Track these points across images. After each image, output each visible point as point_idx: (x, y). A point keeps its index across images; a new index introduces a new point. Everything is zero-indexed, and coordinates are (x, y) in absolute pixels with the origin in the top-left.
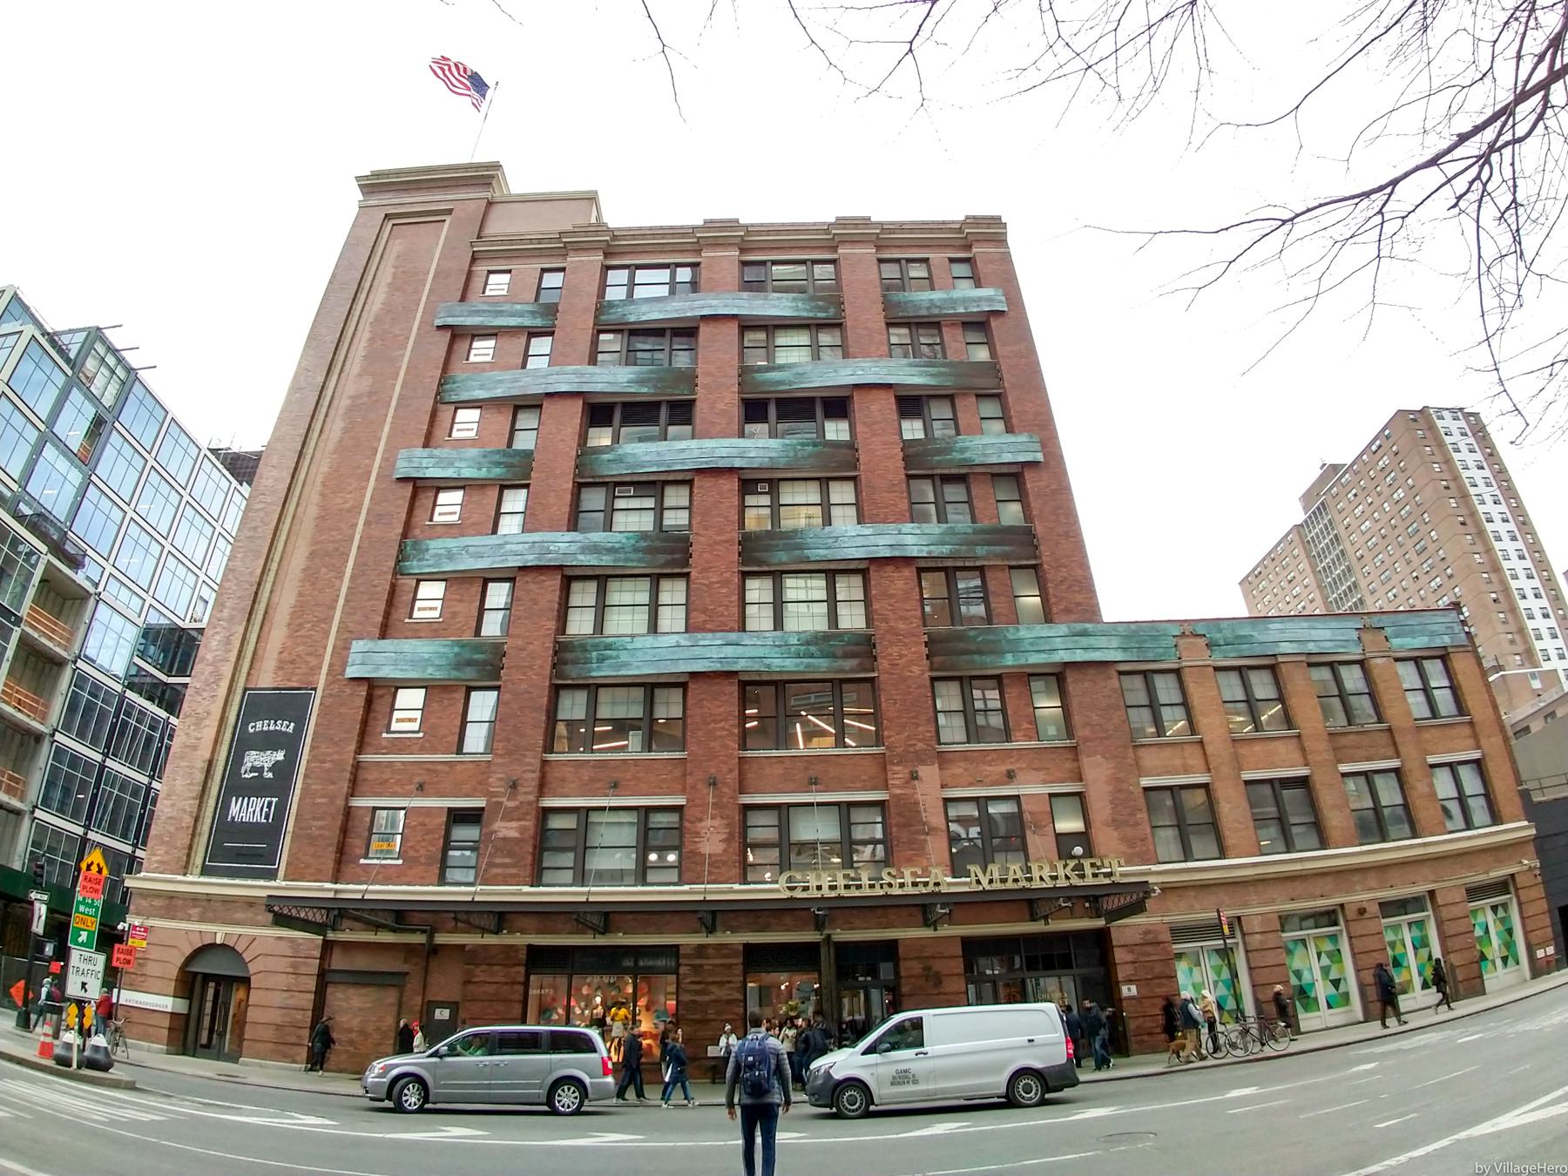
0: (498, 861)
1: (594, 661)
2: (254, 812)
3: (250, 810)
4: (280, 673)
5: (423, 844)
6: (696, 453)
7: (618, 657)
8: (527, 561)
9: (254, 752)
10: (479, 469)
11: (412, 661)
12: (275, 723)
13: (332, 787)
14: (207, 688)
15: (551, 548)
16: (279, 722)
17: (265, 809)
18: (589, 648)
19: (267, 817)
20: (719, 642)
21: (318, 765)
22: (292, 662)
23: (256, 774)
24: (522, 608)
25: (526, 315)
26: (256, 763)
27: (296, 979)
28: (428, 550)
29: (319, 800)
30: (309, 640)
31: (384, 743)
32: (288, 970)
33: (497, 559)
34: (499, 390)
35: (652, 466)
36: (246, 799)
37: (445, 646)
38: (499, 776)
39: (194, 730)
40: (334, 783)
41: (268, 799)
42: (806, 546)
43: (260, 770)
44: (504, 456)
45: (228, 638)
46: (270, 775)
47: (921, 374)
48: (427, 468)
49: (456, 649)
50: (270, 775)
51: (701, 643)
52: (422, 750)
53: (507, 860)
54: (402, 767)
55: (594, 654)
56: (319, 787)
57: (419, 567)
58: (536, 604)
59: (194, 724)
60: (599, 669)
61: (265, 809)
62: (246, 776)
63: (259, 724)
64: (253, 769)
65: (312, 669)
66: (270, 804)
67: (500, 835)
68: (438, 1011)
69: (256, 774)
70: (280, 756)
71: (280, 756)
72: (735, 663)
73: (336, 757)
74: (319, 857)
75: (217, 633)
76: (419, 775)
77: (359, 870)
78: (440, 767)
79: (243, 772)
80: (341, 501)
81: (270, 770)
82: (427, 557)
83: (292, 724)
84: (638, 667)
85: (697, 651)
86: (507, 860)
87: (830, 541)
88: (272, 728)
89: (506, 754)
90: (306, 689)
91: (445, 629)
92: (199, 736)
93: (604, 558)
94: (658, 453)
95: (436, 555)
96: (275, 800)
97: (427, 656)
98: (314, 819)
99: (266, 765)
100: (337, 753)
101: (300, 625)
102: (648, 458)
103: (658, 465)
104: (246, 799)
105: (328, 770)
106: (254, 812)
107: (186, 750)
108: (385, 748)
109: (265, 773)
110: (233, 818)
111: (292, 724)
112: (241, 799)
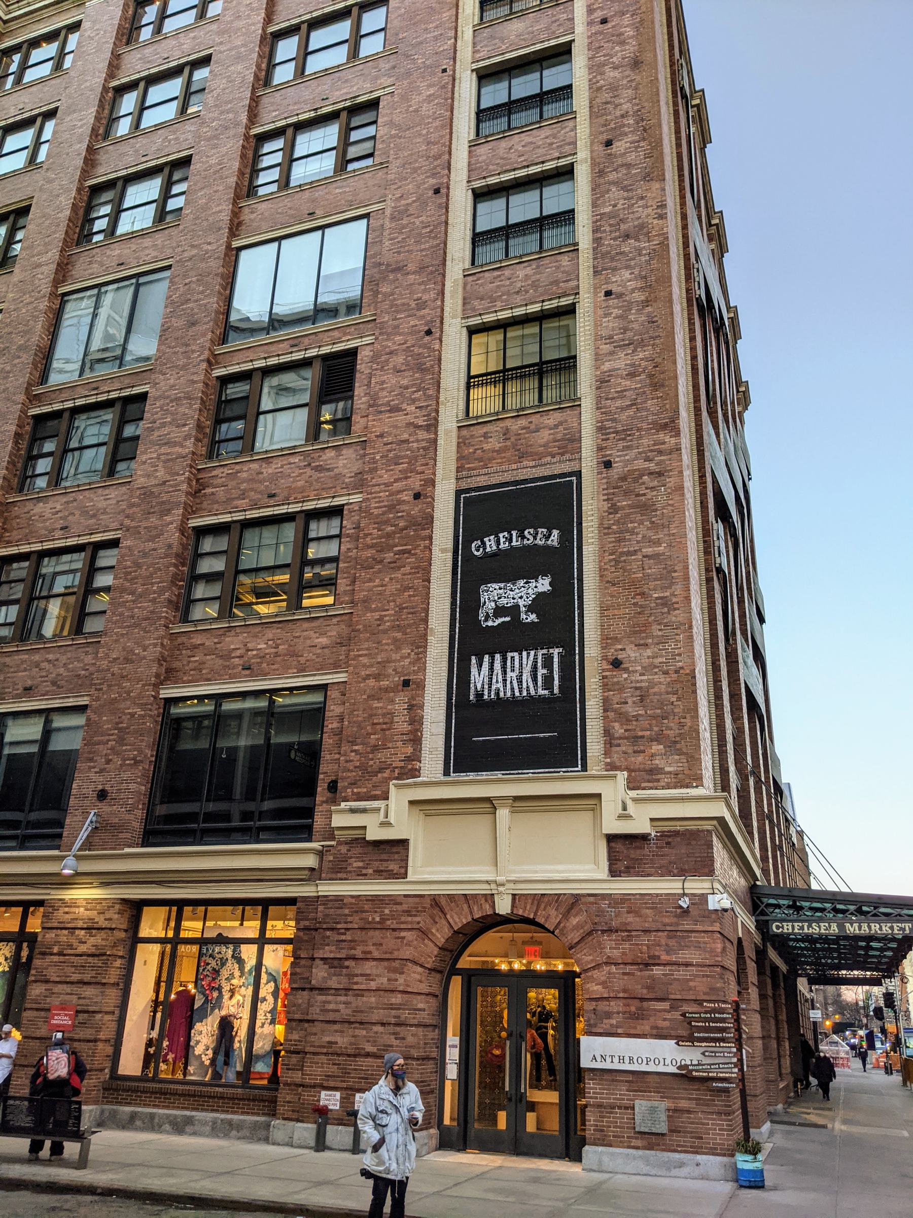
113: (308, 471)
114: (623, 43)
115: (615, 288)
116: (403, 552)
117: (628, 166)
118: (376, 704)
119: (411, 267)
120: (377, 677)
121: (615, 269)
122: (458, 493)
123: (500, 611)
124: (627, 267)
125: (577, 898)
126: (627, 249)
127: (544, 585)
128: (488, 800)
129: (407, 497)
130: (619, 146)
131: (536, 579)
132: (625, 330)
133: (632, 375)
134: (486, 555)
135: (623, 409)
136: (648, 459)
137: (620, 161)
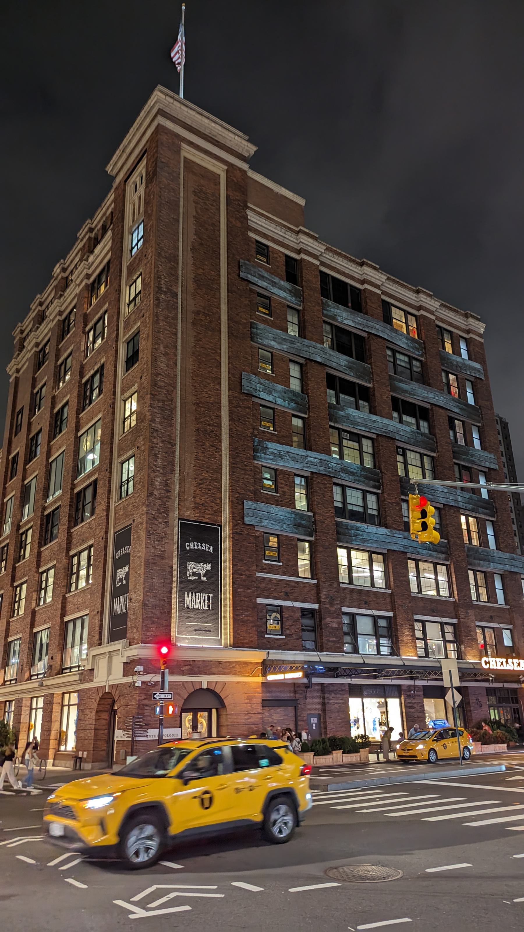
0: (331, 639)
1: (353, 535)
2: (200, 602)
3: (198, 601)
4: (197, 511)
5: (293, 627)
6: (380, 425)
7: (362, 535)
8: (320, 470)
9: (193, 563)
10: (285, 401)
11: (275, 519)
12: (201, 545)
13: (249, 591)
14: (160, 516)
15: (329, 465)
16: (204, 544)
17: (206, 601)
18: (349, 528)
19: (208, 606)
20: (401, 536)
21: (238, 576)
22: (203, 505)
23: (197, 578)
24: (319, 498)
25: (287, 292)
26: (195, 570)
27: (251, 706)
28: (268, 449)
29: (244, 599)
30: (209, 492)
31: (265, 567)
32: (246, 701)
33: (305, 465)
34: (285, 346)
35: (363, 426)
36: (194, 594)
37: (288, 513)
38: (325, 593)
39: (158, 545)
40: (249, 588)
41: (207, 595)
42: (424, 492)
43: (199, 575)
44: (293, 395)
45: (166, 481)
46: (205, 579)
47: (457, 407)
48: (260, 391)
49: (293, 516)
50: (205, 579)
51: (395, 535)
52: (283, 574)
53: (334, 639)
54: (275, 582)
55: (353, 531)
56: (242, 590)
57: (265, 459)
58: (324, 497)
59: (159, 541)
60: (356, 540)
61: (206, 601)
62: (191, 578)
63: (192, 544)
64: (194, 574)
65: (215, 511)
66: (209, 598)
67: (330, 625)
68: (312, 719)
69: (197, 578)
70: (208, 567)
71: (208, 567)
72: (408, 549)
73: (247, 572)
74: (249, 633)
75: (157, 476)
76: (285, 587)
77: (265, 641)
78: (293, 584)
79: (188, 575)
80: (206, 396)
81: (204, 575)
82: (268, 453)
83: (212, 547)
84: (372, 543)
85: (395, 540)
86: (334, 639)
87: (433, 491)
88: (200, 548)
89: (326, 581)
90: (215, 525)
91: (282, 501)
92: (163, 549)
93: (351, 477)
94: (364, 419)
95: (272, 453)
96: (211, 595)
97: (282, 517)
98: (243, 610)
99: (201, 572)
100: (247, 570)
101: (201, 480)
102: (359, 421)
103: (366, 427)
104: (194, 594)
105: (244, 581)
106: (200, 602)
107: (156, 558)
108: (265, 569)
109: (202, 578)
110: (188, 606)
111: (212, 547)
112: (190, 593)
113: (89, 530)
114: (146, 327)
115: (139, 445)
116: (100, 561)
117: (144, 388)
118: (93, 621)
119: (105, 442)
120: (93, 610)
121: (139, 436)
122: (115, 533)
123: (121, 580)
124: (142, 435)
125: (118, 685)
126: (142, 427)
127: (127, 569)
128: (104, 653)
129: (101, 539)
130: (143, 378)
131: (126, 566)
132: (140, 463)
133: (140, 483)
134: (119, 558)
135: (138, 497)
136: (141, 518)
137: (143, 386)
